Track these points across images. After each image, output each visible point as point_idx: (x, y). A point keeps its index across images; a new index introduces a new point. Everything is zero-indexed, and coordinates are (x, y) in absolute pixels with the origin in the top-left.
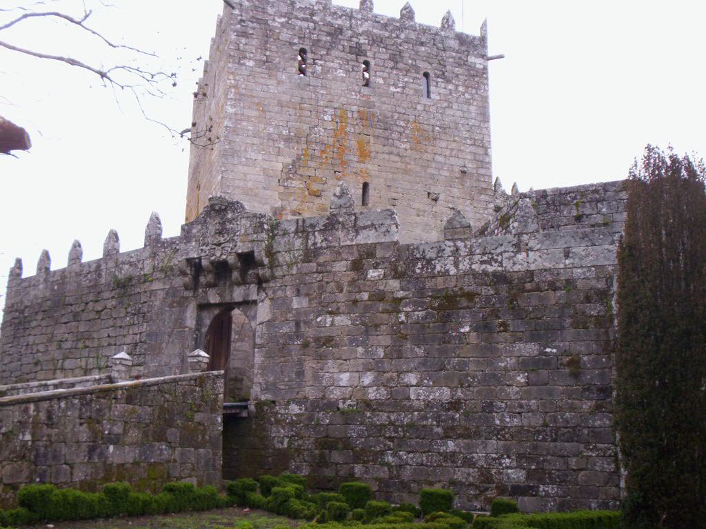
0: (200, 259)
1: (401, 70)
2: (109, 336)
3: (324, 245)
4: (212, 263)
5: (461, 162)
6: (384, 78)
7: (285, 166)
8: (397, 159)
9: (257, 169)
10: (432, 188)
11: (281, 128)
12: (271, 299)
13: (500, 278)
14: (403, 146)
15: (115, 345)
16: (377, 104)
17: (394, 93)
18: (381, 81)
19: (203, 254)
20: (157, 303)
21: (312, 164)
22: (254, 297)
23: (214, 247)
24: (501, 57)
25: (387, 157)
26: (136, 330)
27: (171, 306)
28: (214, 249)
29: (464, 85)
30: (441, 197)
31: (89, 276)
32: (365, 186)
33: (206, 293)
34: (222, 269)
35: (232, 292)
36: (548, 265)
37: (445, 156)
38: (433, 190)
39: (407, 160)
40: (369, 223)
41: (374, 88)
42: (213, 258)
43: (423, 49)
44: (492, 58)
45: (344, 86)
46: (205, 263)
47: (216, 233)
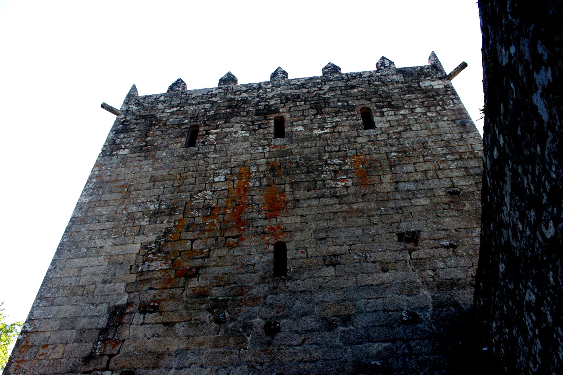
1: (328, 114)
5: (447, 183)
6: (303, 126)
7: (145, 246)
8: (334, 201)
9: (101, 259)
10: (403, 225)
11: (149, 204)
14: (341, 184)
16: (295, 151)
17: (319, 135)
18: (301, 128)
21: (189, 235)
25: (314, 202)
29: (422, 104)
30: (424, 235)
32: (280, 249)
37: (416, 181)
38: (404, 227)
39: (352, 199)
41: (291, 137)
43: (356, 90)
45: (247, 144)
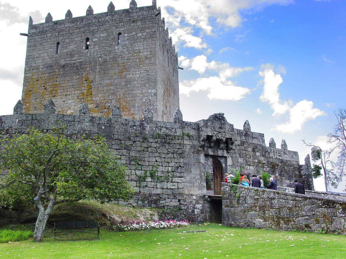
0: (212, 136)
2: (156, 161)
3: (245, 141)
4: (217, 139)
12: (232, 157)
13: (282, 161)
15: (162, 166)
19: (214, 135)
20: (187, 150)
22: (225, 155)
23: (218, 133)
24: (182, 69)
26: (176, 161)
27: (193, 153)
28: (218, 134)
31: (135, 127)
33: (208, 150)
34: (218, 142)
35: (218, 151)
36: (290, 160)
40: (255, 137)
42: (218, 137)
44: (179, 68)
46: (214, 138)
47: (219, 128)
